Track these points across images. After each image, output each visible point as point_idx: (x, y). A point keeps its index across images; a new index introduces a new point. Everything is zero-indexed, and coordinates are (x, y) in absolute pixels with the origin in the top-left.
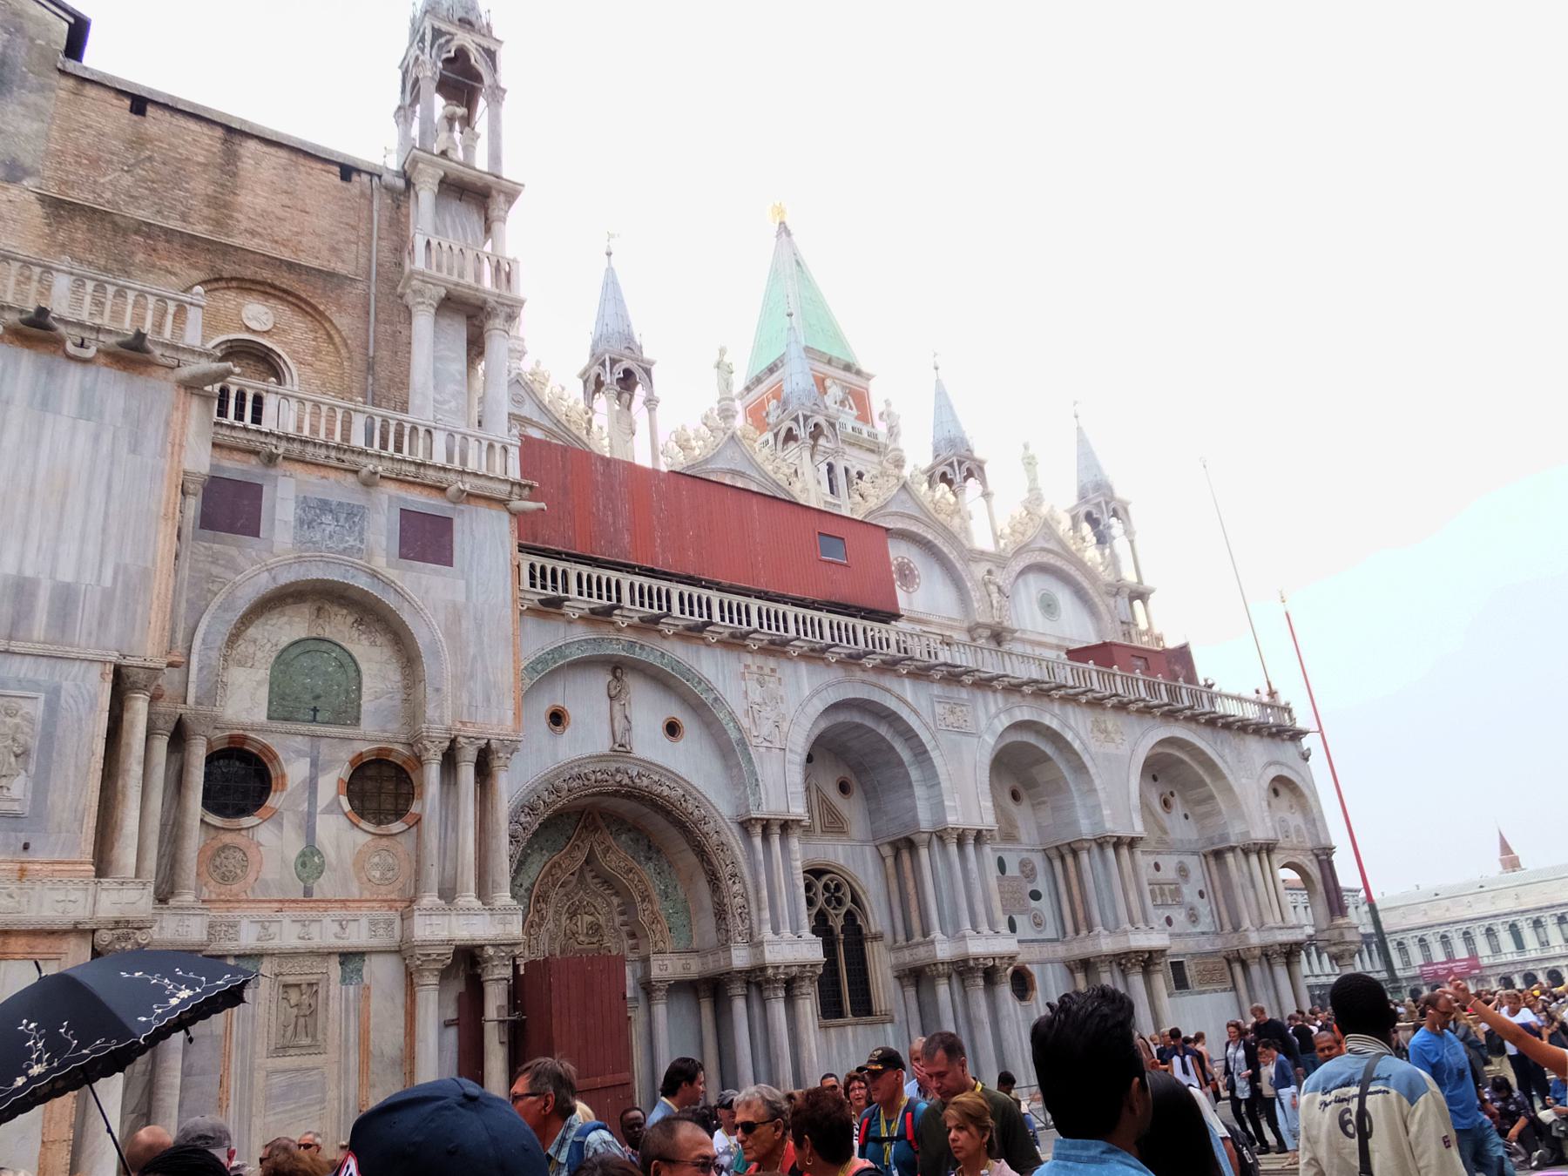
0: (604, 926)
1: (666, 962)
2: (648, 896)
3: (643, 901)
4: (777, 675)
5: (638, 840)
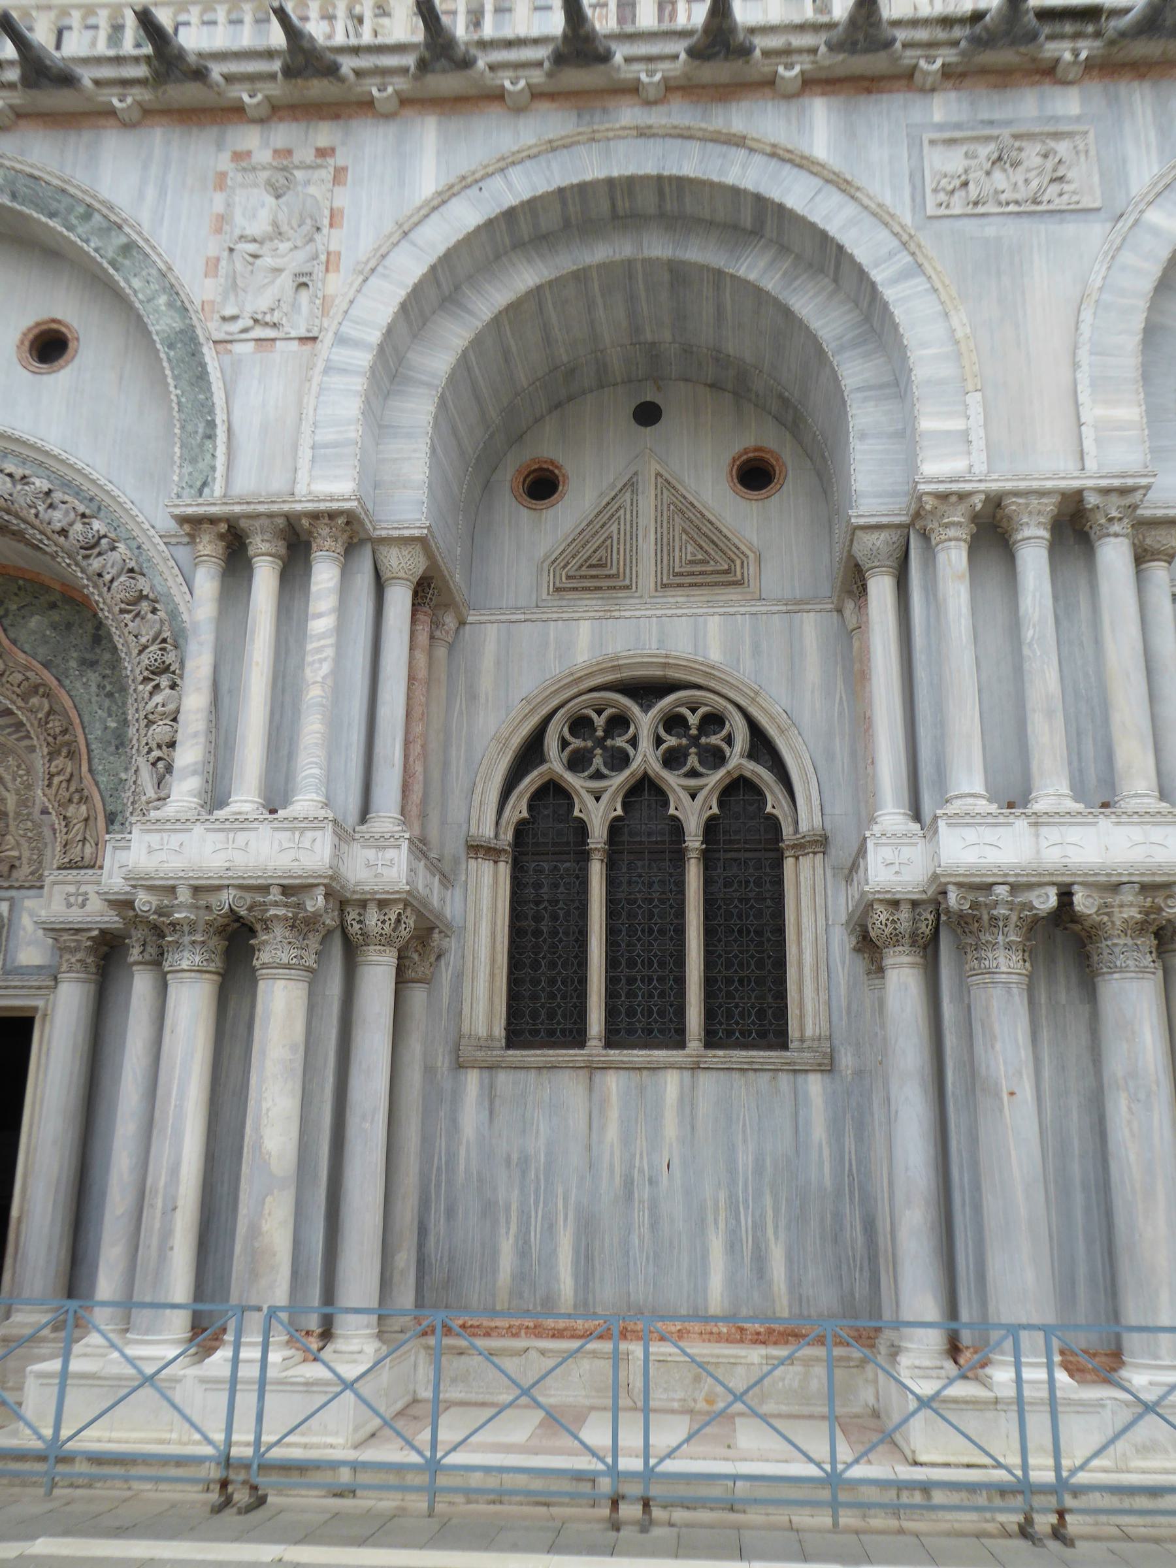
0: (11, 815)
1: (83, 889)
2: (68, 744)
3: (52, 756)
4: (340, 160)
5: (69, 626)
